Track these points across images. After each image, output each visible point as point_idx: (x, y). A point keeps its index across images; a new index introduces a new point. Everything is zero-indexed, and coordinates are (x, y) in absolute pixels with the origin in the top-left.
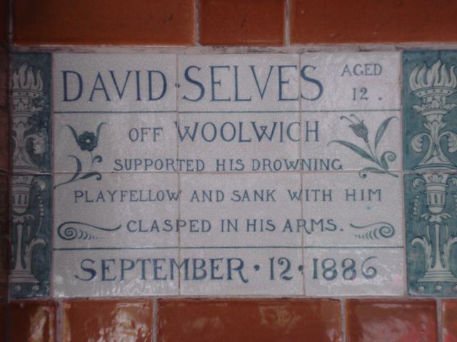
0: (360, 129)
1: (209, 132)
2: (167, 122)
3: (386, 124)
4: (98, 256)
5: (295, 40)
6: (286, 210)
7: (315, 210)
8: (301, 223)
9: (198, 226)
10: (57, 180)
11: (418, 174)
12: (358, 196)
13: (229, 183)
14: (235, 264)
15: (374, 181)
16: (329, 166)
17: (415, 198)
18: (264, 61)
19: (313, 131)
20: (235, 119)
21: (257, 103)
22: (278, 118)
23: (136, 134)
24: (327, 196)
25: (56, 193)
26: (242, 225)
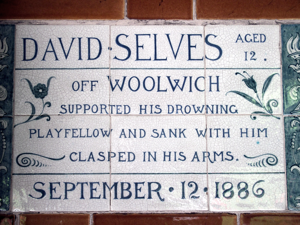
0: (251, 83)
1: (134, 84)
2: (101, 76)
3: (269, 79)
4: (47, 180)
5: (199, 16)
6: (193, 144)
7: (217, 144)
8: (206, 155)
9: (125, 157)
10: (17, 120)
11: (294, 117)
12: (250, 133)
13: (150, 123)
14: (154, 187)
15: (262, 122)
16: (227, 110)
17: (293, 135)
18: (177, 30)
19: (215, 84)
20: (155, 74)
21: (171, 62)
22: (188, 73)
23: (78, 86)
24: (226, 133)
25: (17, 131)
26: (160, 157)
